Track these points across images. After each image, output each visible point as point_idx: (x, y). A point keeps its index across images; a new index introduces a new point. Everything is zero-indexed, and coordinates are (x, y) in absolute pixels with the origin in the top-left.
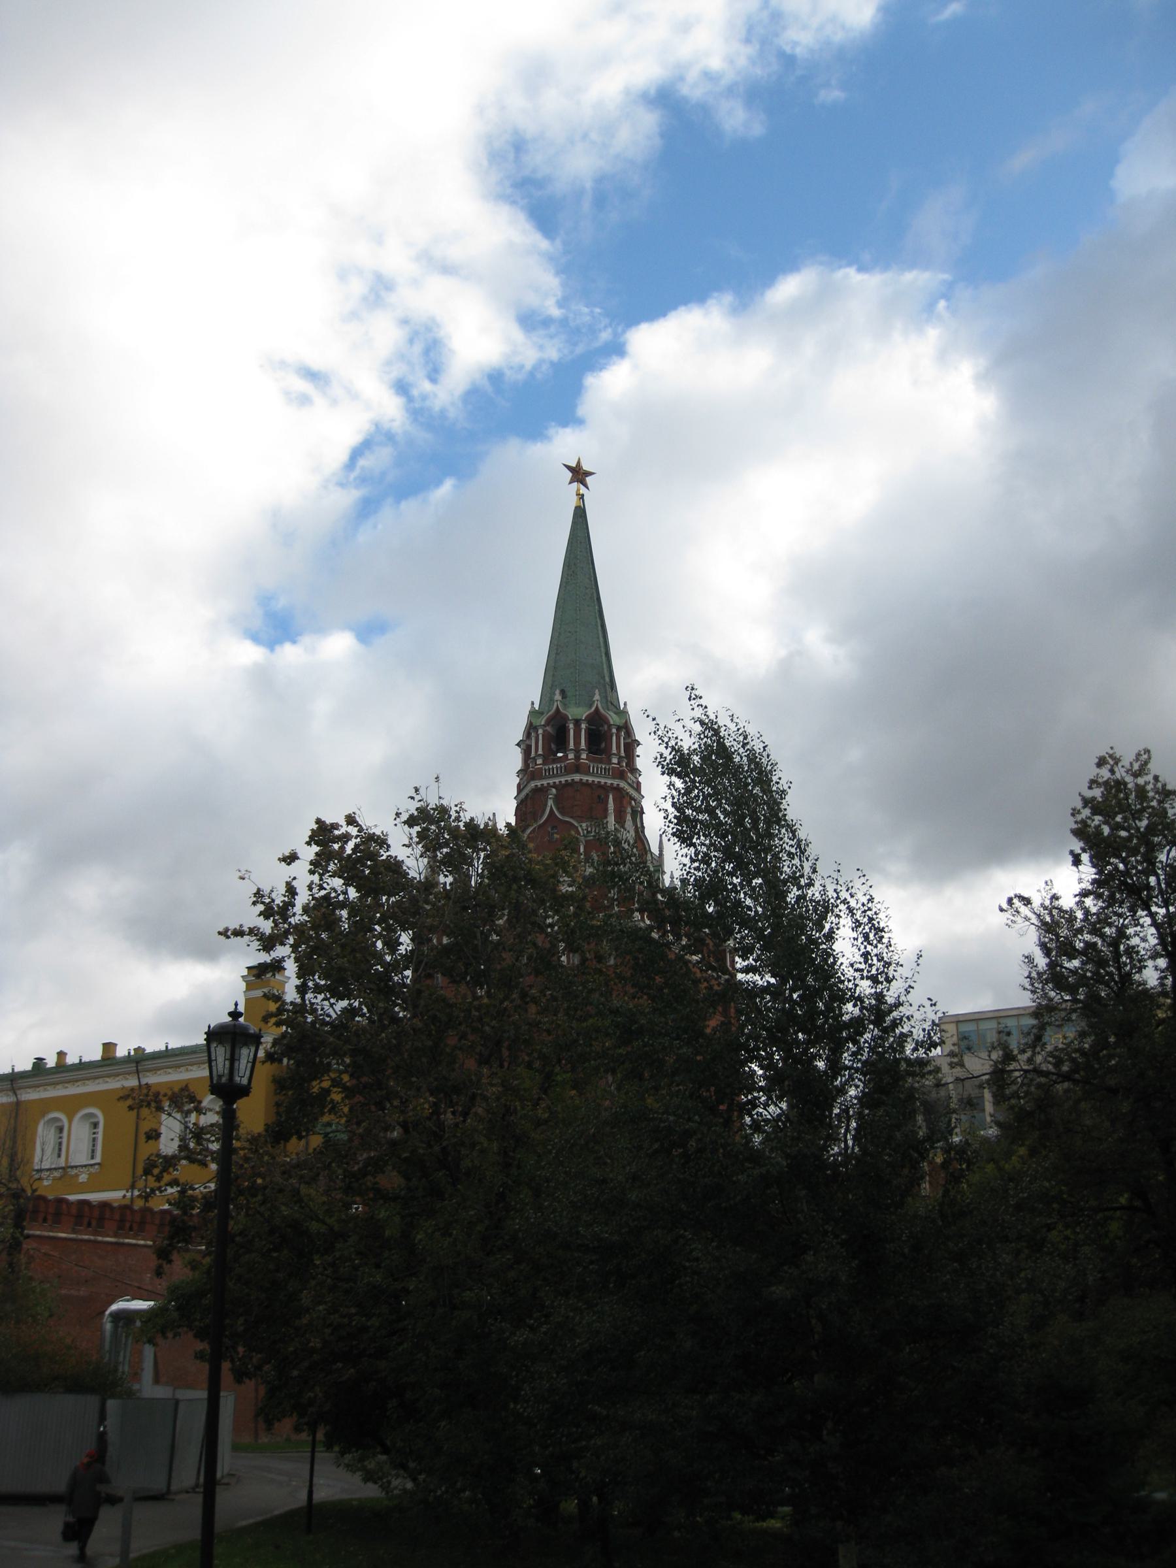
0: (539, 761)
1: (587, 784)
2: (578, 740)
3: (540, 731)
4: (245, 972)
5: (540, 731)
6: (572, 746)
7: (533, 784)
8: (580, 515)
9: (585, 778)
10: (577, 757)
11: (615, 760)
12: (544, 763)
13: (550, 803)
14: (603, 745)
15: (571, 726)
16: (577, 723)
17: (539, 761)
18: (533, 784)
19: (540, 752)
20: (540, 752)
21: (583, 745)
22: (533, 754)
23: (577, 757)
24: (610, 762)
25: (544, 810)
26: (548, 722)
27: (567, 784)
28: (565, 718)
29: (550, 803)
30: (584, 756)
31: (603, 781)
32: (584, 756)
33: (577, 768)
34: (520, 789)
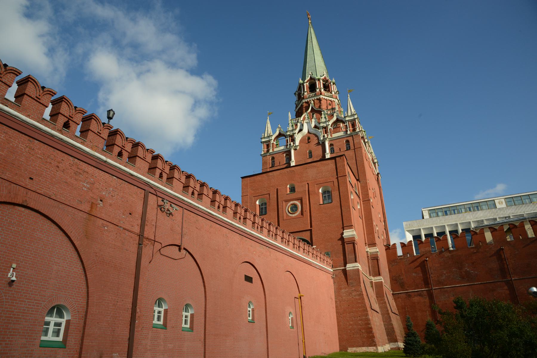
1: (324, 99)
2: (320, 85)
3: (305, 84)
6: (318, 87)
9: (324, 97)
10: (320, 91)
11: (333, 93)
16: (319, 80)
17: (306, 94)
18: (304, 101)
21: (322, 86)
27: (317, 99)
28: (314, 79)
30: (322, 90)
31: (330, 99)
32: (322, 90)
33: (321, 94)
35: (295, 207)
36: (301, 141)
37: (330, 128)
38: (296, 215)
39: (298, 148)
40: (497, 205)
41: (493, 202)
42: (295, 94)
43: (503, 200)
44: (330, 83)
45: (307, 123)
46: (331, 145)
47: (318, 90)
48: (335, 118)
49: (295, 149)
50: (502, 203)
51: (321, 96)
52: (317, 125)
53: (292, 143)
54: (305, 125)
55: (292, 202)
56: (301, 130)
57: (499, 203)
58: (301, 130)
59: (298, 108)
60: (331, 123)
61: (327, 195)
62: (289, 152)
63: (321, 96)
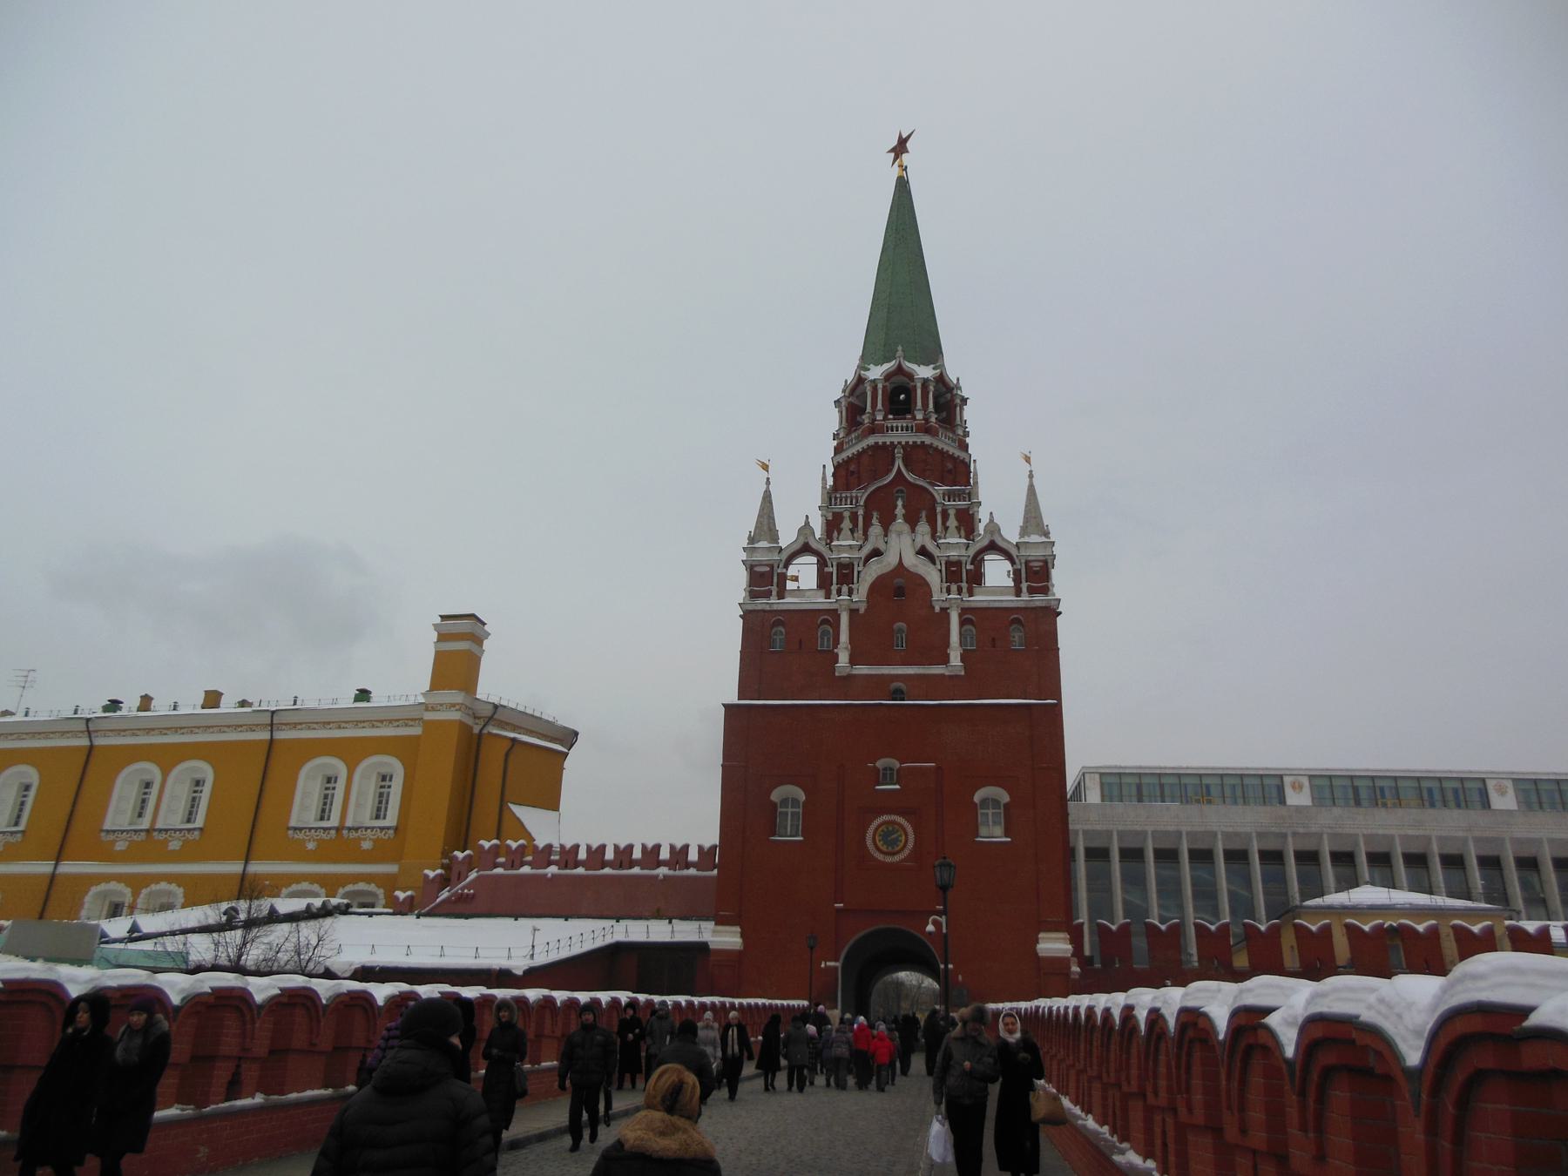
0: (880, 417)
1: (936, 449)
3: (880, 386)
4: (438, 620)
5: (880, 386)
7: (871, 440)
8: (903, 187)
9: (936, 443)
10: (926, 420)
12: (885, 418)
13: (899, 463)
14: (944, 414)
15: (919, 385)
16: (925, 382)
17: (880, 417)
18: (871, 440)
19: (880, 406)
20: (880, 406)
22: (869, 409)
23: (926, 420)
24: (954, 432)
25: (889, 471)
26: (888, 377)
29: (899, 463)
33: (926, 429)
34: (838, 450)
35: (889, 836)
36: (875, 588)
37: (969, 567)
38: (897, 858)
39: (862, 611)
40: (1288, 791)
41: (1277, 781)
42: (837, 403)
43: (1305, 781)
44: (952, 400)
45: (899, 534)
46: (962, 623)
47: (919, 416)
48: (981, 542)
49: (853, 613)
50: (1301, 787)
51: (927, 440)
52: (931, 547)
53: (845, 589)
54: (893, 537)
55: (885, 818)
56: (876, 553)
57: (1293, 787)
58: (876, 553)
59: (844, 455)
60: (971, 552)
61: (990, 812)
62: (835, 614)
63: (927, 440)
